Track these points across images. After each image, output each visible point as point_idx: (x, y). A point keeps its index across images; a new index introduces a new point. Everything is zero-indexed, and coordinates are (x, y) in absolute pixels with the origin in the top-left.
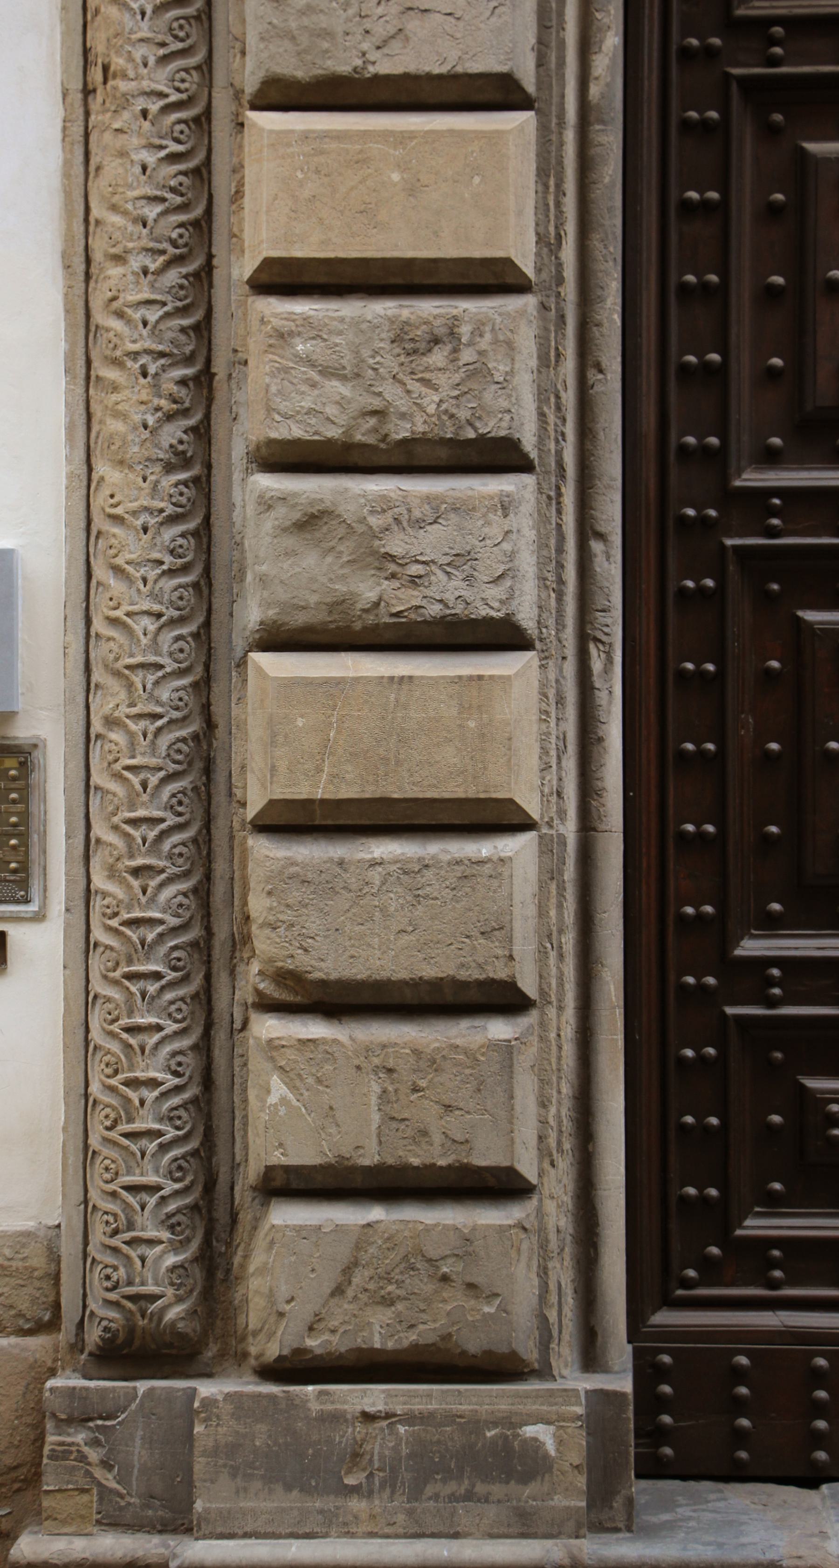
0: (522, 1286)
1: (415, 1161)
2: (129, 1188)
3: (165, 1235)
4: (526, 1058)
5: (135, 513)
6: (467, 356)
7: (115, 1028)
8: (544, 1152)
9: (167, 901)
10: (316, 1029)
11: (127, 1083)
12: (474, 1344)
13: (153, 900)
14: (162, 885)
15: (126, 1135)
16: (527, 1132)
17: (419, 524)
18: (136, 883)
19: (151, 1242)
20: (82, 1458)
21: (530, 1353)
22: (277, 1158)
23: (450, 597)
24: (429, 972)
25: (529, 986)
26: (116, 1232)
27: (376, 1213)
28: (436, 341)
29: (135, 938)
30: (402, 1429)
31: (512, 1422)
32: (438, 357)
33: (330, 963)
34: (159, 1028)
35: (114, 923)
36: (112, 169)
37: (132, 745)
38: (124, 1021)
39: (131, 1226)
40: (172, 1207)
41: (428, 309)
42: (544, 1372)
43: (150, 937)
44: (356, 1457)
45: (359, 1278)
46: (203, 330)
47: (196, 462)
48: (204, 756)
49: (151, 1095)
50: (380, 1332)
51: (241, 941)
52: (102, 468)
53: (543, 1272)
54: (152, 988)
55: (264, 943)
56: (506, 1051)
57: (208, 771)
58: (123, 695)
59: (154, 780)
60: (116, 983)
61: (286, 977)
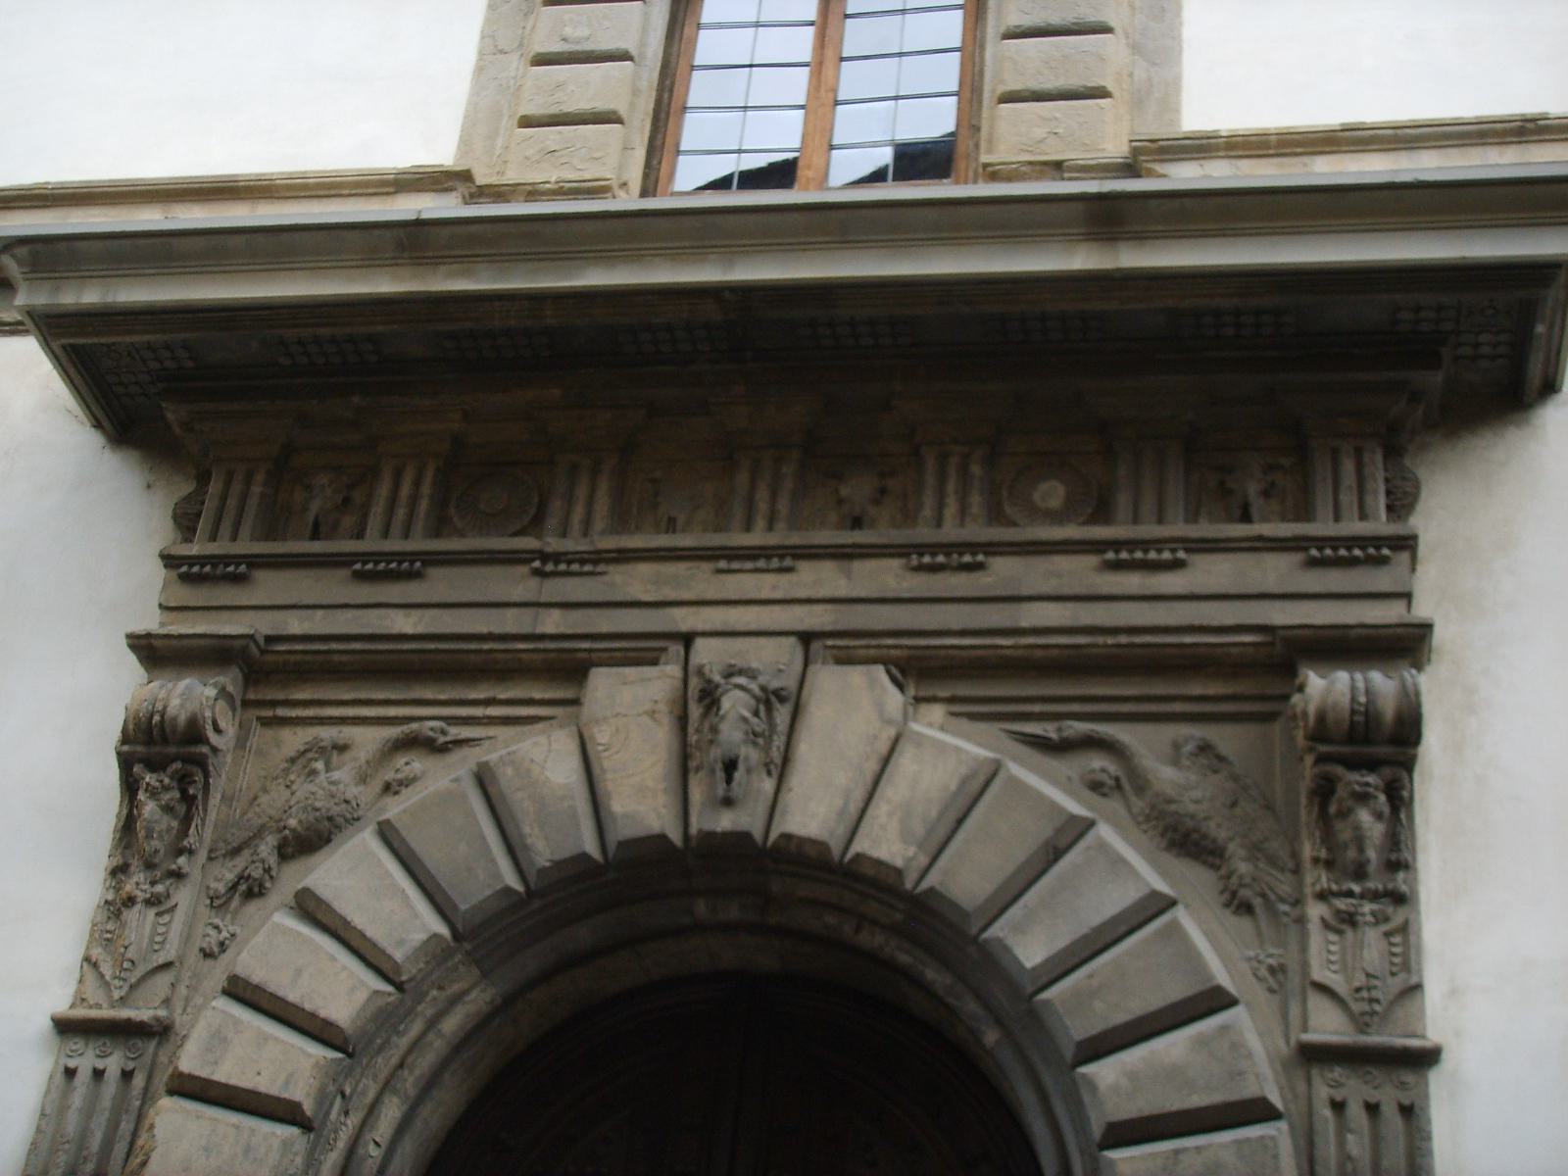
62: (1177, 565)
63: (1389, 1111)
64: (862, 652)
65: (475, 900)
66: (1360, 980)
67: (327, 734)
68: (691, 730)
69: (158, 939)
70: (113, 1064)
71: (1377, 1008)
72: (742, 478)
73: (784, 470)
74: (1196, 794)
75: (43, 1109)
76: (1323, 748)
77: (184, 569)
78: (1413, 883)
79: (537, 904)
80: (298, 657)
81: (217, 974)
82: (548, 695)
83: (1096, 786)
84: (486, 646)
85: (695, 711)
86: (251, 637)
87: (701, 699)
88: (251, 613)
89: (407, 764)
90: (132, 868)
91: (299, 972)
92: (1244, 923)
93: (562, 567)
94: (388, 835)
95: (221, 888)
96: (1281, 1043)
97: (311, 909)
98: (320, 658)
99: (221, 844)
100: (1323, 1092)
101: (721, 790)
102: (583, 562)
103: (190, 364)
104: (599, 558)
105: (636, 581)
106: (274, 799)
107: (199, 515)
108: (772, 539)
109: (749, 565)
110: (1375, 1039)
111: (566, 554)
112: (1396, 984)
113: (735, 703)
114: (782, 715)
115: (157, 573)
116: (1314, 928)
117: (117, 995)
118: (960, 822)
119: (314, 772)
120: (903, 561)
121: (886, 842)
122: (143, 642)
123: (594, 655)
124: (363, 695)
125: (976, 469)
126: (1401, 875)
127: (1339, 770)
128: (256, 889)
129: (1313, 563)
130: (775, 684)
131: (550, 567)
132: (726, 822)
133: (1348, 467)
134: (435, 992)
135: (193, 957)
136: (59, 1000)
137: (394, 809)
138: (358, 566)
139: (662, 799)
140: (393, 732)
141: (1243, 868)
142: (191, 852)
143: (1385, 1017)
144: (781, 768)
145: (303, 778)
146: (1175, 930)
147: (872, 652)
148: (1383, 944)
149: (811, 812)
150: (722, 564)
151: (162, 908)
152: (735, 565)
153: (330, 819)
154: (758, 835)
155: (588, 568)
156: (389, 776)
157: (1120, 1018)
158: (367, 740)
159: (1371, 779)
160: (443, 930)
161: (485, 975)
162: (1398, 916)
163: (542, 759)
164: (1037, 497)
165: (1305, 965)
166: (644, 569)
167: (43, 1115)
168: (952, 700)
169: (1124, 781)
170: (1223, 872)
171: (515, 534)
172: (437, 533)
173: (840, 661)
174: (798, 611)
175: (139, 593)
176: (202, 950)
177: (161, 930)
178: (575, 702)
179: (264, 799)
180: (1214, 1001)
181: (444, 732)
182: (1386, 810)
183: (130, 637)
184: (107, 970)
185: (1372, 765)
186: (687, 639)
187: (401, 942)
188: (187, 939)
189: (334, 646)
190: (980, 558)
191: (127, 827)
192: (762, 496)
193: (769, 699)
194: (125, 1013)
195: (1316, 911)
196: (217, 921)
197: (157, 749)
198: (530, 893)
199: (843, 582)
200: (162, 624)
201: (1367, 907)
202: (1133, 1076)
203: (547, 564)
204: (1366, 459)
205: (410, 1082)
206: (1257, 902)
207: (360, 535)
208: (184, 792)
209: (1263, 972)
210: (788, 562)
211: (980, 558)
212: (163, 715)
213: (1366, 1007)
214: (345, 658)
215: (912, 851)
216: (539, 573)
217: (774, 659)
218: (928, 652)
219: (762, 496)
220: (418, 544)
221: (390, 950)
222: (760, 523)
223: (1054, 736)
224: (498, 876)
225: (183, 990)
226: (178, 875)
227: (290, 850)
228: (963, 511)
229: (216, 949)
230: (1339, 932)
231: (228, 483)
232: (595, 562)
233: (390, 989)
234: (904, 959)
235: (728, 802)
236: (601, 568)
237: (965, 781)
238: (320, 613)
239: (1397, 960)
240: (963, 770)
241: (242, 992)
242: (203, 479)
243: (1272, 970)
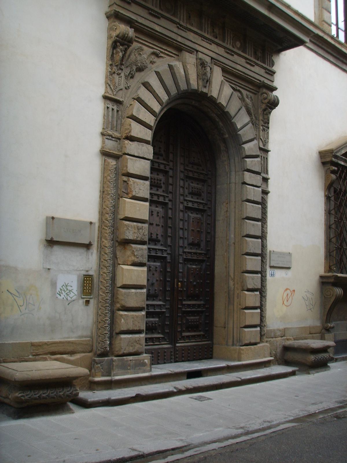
1: (135, 329)
3: (108, 339)
5: (108, 246)
19: (107, 340)
20: (100, 368)
23: (141, 260)
24: (137, 306)
27: (130, 336)
30: (134, 362)
37: (107, 276)
38: (105, 312)
39: (105, 338)
41: (140, 225)
48: (113, 279)
58: (106, 270)
82: (174, 53)
84: (169, 39)
105: (191, 36)
109: (206, 41)
111: (183, 25)
122: (117, 13)
123: (184, 48)
124: (146, 40)
129: (266, 73)
151: (119, 76)
152: (204, 40)
158: (149, 51)
166: (192, 34)
174: (212, 53)
178: (178, 56)
186: (197, 51)
189: (145, 28)
210: (211, 43)
212: (128, 35)
216: (178, 27)
236: (186, 31)
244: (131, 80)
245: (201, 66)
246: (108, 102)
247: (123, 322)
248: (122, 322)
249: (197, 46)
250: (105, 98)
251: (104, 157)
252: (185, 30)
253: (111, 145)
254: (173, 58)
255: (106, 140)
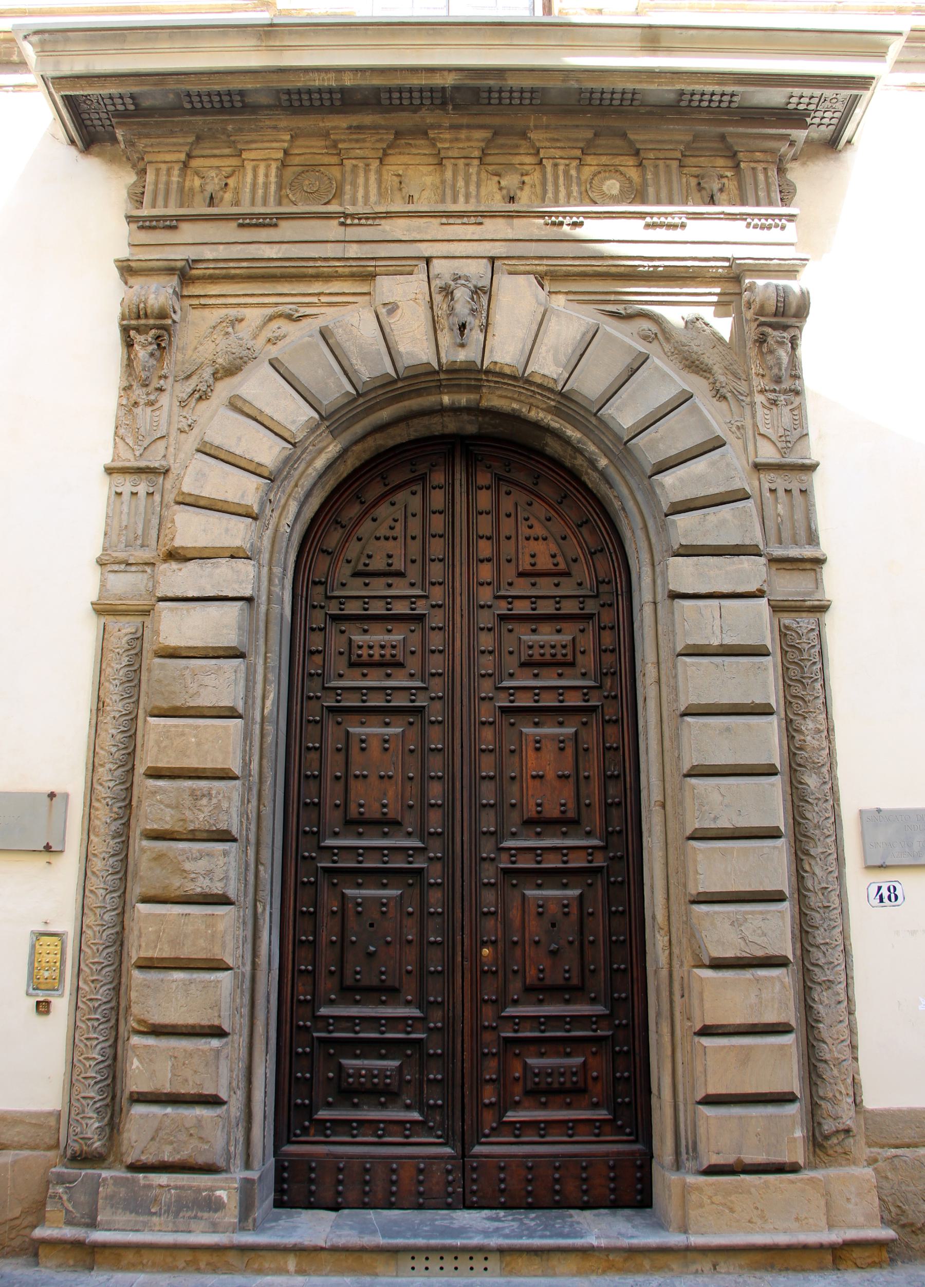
0: (218, 1140)
1: (183, 1091)
2: (84, 1098)
3: (95, 1115)
4: (223, 1054)
5: (101, 853)
6: (214, 801)
7: (82, 1038)
8: (230, 1088)
9: (102, 994)
10: (151, 1041)
11: (85, 1059)
12: (201, 1160)
13: (98, 992)
14: (101, 986)
15: (84, 1078)
16: (224, 1081)
17: (196, 859)
18: (93, 985)
19: (90, 1118)
20: (61, 1198)
21: (221, 1163)
22: (134, 1088)
23: (204, 886)
25: (226, 1027)
26: (78, 1114)
27: (169, 1110)
28: (204, 796)
29: (91, 1005)
30: (173, 1191)
31: (212, 1189)
32: (204, 801)
33: (157, 1018)
34: (97, 1039)
35: (84, 1000)
36: (103, 734)
37: (95, 935)
38: (85, 1036)
40: (98, 1105)
42: (227, 1170)
43: (96, 1005)
44: (156, 1200)
45: (162, 1134)
46: (130, 789)
47: (123, 835)
48: (119, 941)
49: (93, 1063)
50: (167, 1156)
51: (128, 1008)
52: (92, 837)
53: (229, 1133)
54: (96, 1024)
55: (135, 1009)
56: (217, 1052)
57: (122, 945)
58: (93, 918)
59: (101, 948)
60: (83, 1021)
61: (141, 1022)
62: (683, 226)
63: (796, 493)
64: (522, 268)
65: (331, 399)
66: (781, 432)
67: (233, 313)
68: (434, 307)
69: (155, 424)
70: (142, 489)
71: (789, 445)
72: (449, 174)
73: (471, 170)
74: (697, 342)
75: (107, 514)
76: (763, 319)
77: (141, 223)
78: (802, 385)
79: (361, 400)
80: (211, 271)
81: (191, 442)
83: (645, 338)
85: (438, 298)
86: (187, 260)
87: (440, 292)
88: (182, 247)
89: (279, 328)
90: (134, 387)
91: (239, 439)
92: (724, 405)
93: (356, 221)
94: (274, 364)
95: (185, 396)
96: (745, 462)
97: (237, 405)
98: (224, 271)
99: (181, 373)
100: (766, 486)
101: (458, 341)
102: (367, 218)
103: (132, 107)
104: (377, 216)
106: (207, 351)
107: (143, 193)
108: (470, 208)
109: (459, 221)
110: (788, 460)
112: (796, 434)
113: (462, 295)
114: (484, 300)
115: (124, 228)
116: (759, 407)
117: (137, 453)
118: (582, 355)
119: (227, 333)
120: (541, 221)
121: (547, 366)
122: (125, 264)
125: (573, 172)
126: (797, 382)
127: (770, 330)
128: (204, 397)
130: (480, 285)
131: (349, 221)
132: (462, 356)
133: (761, 177)
134: (311, 448)
135: (174, 433)
136: (107, 458)
137: (274, 351)
138: (241, 221)
139: (426, 344)
140: (269, 311)
141: (722, 378)
142: (166, 377)
143: (791, 449)
144: (485, 328)
145: (221, 337)
146: (695, 410)
147: (528, 268)
148: (790, 415)
149: (505, 350)
150: (444, 220)
152: (451, 221)
153: (241, 358)
154: (479, 364)
155: (370, 222)
156: (270, 335)
157: (673, 452)
158: (254, 316)
159: (785, 335)
160: (316, 416)
161: (335, 438)
162: (797, 401)
163: (357, 324)
164: (605, 188)
165: (755, 425)
166: (402, 222)
167: (107, 516)
168: (567, 293)
169: (659, 335)
170: (711, 380)
171: (325, 204)
172: (280, 204)
173: (510, 273)
175: (113, 238)
176: (179, 429)
177: (157, 419)
178: (369, 294)
179: (201, 348)
180: (717, 444)
181: (297, 311)
182: (789, 349)
183: (116, 261)
184: (130, 441)
185: (785, 328)
186: (428, 260)
187: (294, 422)
188: (169, 424)
189: (232, 265)
190: (581, 219)
191: (129, 364)
192: (461, 183)
193: (477, 291)
194: (142, 464)
195: (759, 399)
196: (184, 414)
197: (143, 322)
198: (359, 395)
199: (509, 231)
200: (132, 254)
201: (782, 397)
202: (681, 480)
203: (345, 219)
204: (769, 174)
205: (300, 492)
206: (728, 395)
207: (237, 203)
208: (159, 345)
209: (734, 429)
210: (480, 220)
211: (581, 219)
213: (784, 445)
214: (238, 271)
215: (560, 370)
216: (343, 224)
217: (477, 270)
218: (557, 268)
219: (461, 183)
220: (272, 209)
221: (289, 427)
222: (462, 199)
223: (623, 312)
224: (342, 386)
225: (171, 450)
226: (161, 390)
227: (219, 375)
228: (569, 195)
229: (187, 429)
230: (770, 409)
231: (157, 175)
232: (374, 218)
233: (290, 446)
234: (556, 425)
235: (462, 345)
236: (377, 221)
237: (584, 334)
238: (221, 247)
239: (796, 422)
240: (583, 329)
241: (208, 451)
242: (142, 172)
243: (738, 428)
244: (203, 405)
245: (444, 293)
246: (118, 478)
247: (138, 1067)
248: (134, 1067)
249: (422, 246)
250: (110, 471)
251: (103, 620)
252: (356, 221)
253: (126, 584)
254: (350, 307)
255: (112, 576)
